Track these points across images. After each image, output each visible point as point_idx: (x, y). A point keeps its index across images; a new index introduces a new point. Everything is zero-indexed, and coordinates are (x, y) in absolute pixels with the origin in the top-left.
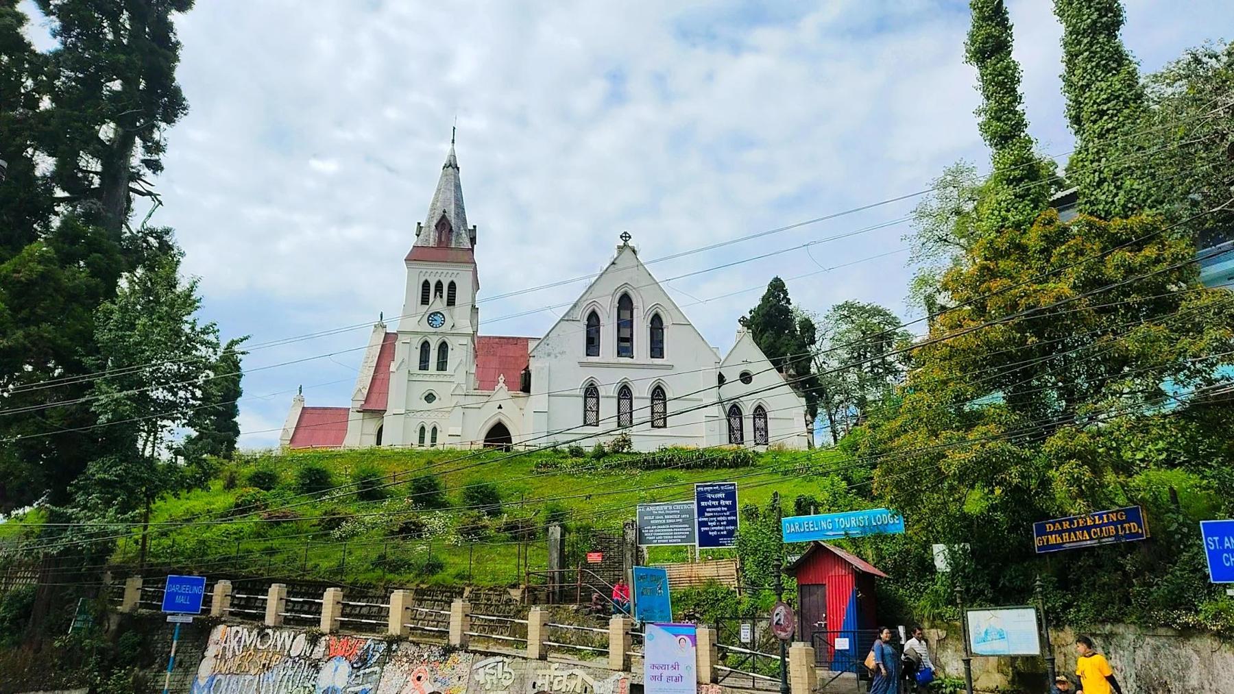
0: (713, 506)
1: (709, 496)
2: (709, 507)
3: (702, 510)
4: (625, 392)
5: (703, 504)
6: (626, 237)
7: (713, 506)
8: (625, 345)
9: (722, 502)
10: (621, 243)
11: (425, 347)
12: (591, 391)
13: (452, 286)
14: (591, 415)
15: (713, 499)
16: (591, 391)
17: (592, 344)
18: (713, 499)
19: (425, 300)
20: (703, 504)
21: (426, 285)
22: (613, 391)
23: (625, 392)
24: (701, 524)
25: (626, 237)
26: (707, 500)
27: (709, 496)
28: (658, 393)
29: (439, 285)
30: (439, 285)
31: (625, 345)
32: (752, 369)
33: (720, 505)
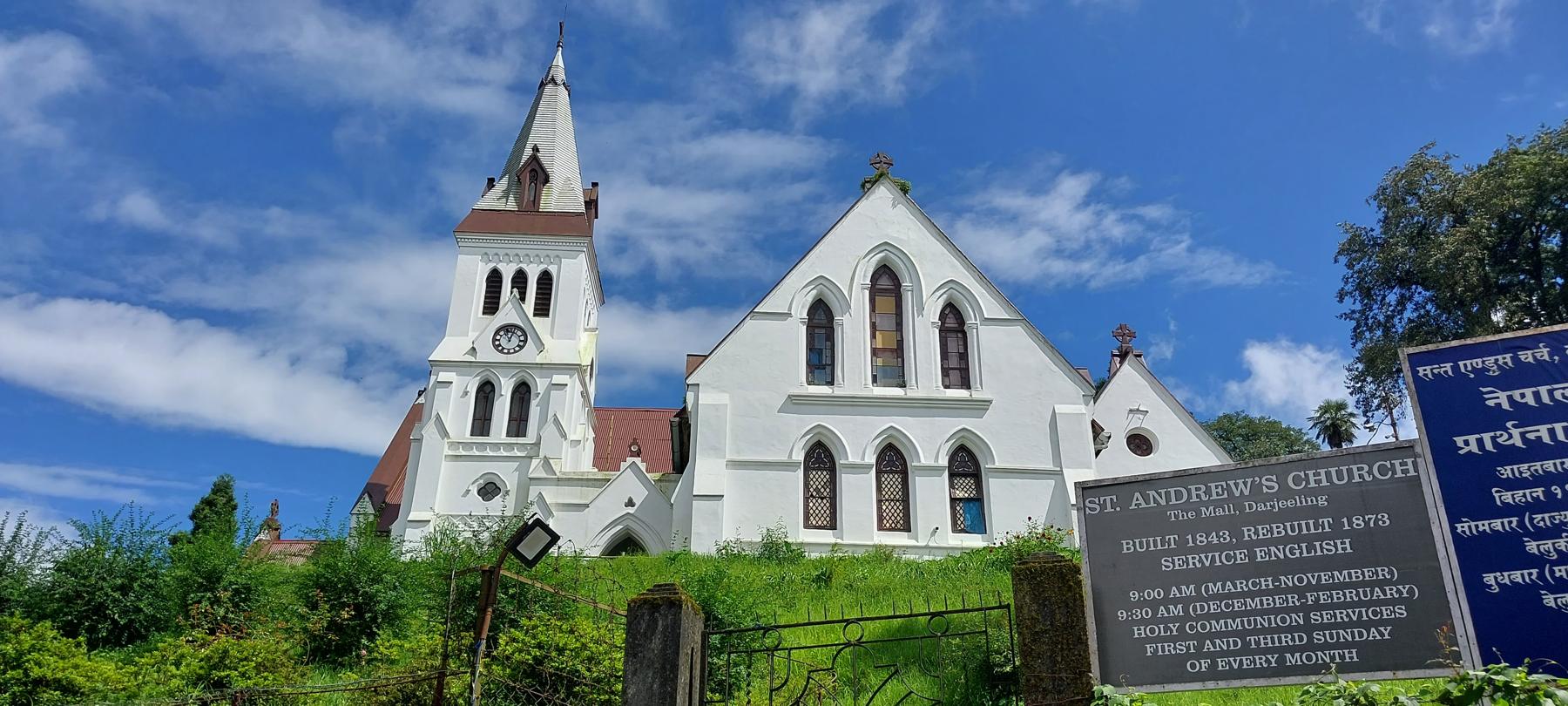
0: (1535, 450)
2: (1509, 455)
3: (1468, 487)
4: (893, 460)
5: (1468, 444)
8: (891, 361)
11: (486, 392)
12: (821, 458)
13: (546, 280)
14: (823, 503)
16: (821, 458)
17: (821, 362)
19: (491, 306)
20: (1468, 444)
21: (494, 279)
23: (893, 460)
28: (965, 463)
29: (520, 280)
30: (520, 280)
31: (891, 361)
32: (1148, 425)
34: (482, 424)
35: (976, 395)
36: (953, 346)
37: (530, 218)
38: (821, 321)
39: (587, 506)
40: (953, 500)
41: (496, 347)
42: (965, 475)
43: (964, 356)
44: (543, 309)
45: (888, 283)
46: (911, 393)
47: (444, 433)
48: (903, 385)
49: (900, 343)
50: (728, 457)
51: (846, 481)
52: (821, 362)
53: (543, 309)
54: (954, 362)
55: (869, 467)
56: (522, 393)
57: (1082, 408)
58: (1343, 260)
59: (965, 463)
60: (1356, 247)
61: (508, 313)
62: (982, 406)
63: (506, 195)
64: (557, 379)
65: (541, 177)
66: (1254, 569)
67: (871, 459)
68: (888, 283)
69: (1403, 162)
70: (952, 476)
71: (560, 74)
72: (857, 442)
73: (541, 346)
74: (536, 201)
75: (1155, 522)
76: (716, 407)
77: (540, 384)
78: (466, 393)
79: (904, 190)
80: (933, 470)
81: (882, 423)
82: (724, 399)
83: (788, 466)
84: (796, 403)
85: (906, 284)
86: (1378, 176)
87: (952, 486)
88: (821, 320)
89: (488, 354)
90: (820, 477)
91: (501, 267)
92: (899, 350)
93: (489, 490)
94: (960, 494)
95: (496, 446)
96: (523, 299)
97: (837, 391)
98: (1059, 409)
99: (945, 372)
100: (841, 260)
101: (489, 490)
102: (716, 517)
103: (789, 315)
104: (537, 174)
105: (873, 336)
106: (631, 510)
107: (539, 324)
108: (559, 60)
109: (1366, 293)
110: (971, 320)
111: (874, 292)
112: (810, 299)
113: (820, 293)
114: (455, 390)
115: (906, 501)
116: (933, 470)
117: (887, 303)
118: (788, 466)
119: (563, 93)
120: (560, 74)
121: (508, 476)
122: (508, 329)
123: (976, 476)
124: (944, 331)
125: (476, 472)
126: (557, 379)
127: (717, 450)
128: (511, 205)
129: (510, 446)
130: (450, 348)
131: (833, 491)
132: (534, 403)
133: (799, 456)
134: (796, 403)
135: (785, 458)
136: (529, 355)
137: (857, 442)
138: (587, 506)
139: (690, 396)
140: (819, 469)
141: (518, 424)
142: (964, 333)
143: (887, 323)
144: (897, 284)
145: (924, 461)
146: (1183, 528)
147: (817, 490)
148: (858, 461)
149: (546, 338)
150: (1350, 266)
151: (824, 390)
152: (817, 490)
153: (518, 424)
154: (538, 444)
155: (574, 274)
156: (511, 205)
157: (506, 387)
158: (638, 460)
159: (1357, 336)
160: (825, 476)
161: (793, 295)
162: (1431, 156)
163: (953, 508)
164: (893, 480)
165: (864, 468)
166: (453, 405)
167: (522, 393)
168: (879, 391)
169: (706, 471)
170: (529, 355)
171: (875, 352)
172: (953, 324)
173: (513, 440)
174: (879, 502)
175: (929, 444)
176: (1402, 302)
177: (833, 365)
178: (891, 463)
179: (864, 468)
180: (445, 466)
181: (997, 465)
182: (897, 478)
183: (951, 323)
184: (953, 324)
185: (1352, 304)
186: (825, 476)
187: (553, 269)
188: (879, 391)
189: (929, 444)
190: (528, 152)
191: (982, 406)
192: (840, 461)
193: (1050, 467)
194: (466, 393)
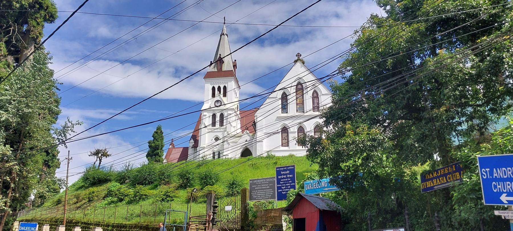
1: (282, 173)
2: (282, 178)
3: (279, 181)
5: (279, 177)
6: (299, 55)
7: (284, 178)
9: (288, 176)
10: (296, 58)
11: (214, 116)
13: (225, 88)
15: (284, 175)
17: (284, 108)
18: (284, 175)
19: (214, 95)
20: (279, 177)
21: (214, 88)
22: (295, 129)
24: (279, 188)
25: (299, 55)
26: (281, 175)
27: (282, 173)
29: (219, 88)
30: (219, 88)
33: (287, 178)
34: (214, 124)
36: (316, 101)
37: (220, 73)
38: (284, 97)
44: (225, 95)
52: (284, 108)
56: (222, 116)
61: (217, 98)
64: (230, 112)
66: (262, 189)
68: (300, 88)
74: (221, 68)
75: (255, 184)
77: (225, 114)
88: (284, 97)
90: (285, 135)
91: (215, 86)
96: (220, 93)
101: (217, 139)
102: (262, 146)
107: (225, 100)
122: (217, 101)
125: (213, 135)
128: (216, 70)
130: (205, 106)
134: (279, 119)
141: (222, 124)
146: (257, 185)
151: (285, 115)
153: (222, 124)
156: (216, 70)
166: (207, 121)
167: (222, 116)
168: (298, 114)
183: (315, 95)
188: (298, 114)
190: (218, 56)
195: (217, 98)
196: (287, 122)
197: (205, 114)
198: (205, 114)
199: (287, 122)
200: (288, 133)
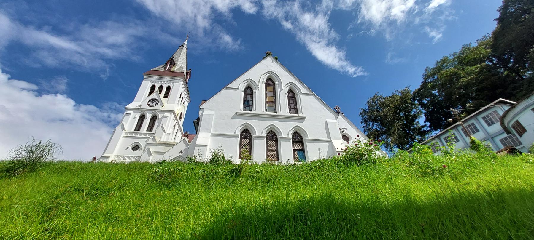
4: (272, 136)
8: (272, 103)
11: (142, 118)
12: (246, 135)
13: (169, 89)
16: (246, 135)
17: (248, 103)
21: (153, 87)
23: (272, 136)
28: (298, 138)
29: (161, 88)
30: (161, 88)
31: (272, 103)
34: (139, 127)
35: (300, 115)
36: (292, 102)
38: (249, 92)
39: (165, 153)
40: (294, 150)
41: (148, 105)
42: (298, 142)
43: (296, 105)
44: (166, 96)
45: (271, 83)
46: (278, 114)
47: (123, 129)
48: (276, 112)
49: (275, 100)
50: (212, 132)
51: (255, 142)
52: (248, 103)
53: (166, 96)
54: (292, 106)
55: (264, 137)
57: (335, 121)
58: (361, 116)
59: (298, 138)
60: (363, 113)
61: (154, 96)
62: (303, 119)
63: (162, 68)
64: (166, 114)
65: (173, 63)
67: (265, 135)
68: (271, 83)
69: (372, 96)
70: (293, 142)
71: (185, 45)
72: (260, 129)
73: (162, 105)
76: (209, 115)
77: (160, 116)
78: (135, 117)
79: (276, 59)
80: (287, 139)
81: (269, 123)
82: (213, 113)
83: (234, 136)
84: (238, 115)
85: (277, 82)
86: (367, 100)
87: (293, 146)
88: (249, 92)
89: (145, 106)
90: (245, 141)
91: (156, 84)
92: (274, 102)
93: (136, 148)
94: (296, 148)
95: (141, 134)
96: (160, 93)
97: (253, 112)
98: (328, 121)
99: (290, 109)
100: (258, 73)
101: (136, 148)
103: (238, 89)
104: (173, 64)
105: (266, 98)
106: (181, 154)
107: (164, 100)
108: (186, 42)
109: (366, 122)
110: (297, 93)
111: (267, 85)
112: (246, 85)
113: (249, 84)
114: (131, 117)
115: (277, 150)
116: (287, 139)
117: (270, 88)
118: (234, 136)
119: (185, 50)
120: (185, 45)
121: (142, 143)
122: (153, 100)
123: (302, 142)
124: (289, 98)
126: (166, 114)
127: (207, 130)
128: (163, 69)
129: (146, 134)
131: (251, 146)
132: (157, 121)
133: (239, 133)
134: (238, 115)
135: (233, 133)
136: (158, 107)
137: (260, 129)
138: (165, 153)
139: (200, 112)
140: (246, 138)
141: (151, 128)
142: (295, 98)
143: (271, 94)
144: (274, 83)
145: (283, 136)
147: (245, 146)
148: (260, 135)
149: (165, 104)
150: (362, 117)
152: (245, 146)
153: (151, 128)
154: (155, 134)
155: (179, 88)
156: (163, 69)
157: (149, 117)
158: (186, 138)
159: (365, 131)
160: (248, 141)
161: (240, 83)
162: (378, 95)
163: (294, 153)
164: (272, 143)
165: (262, 138)
168: (267, 113)
169: (203, 137)
170: (158, 107)
171: (266, 102)
172: (292, 96)
173: (148, 132)
174: (267, 150)
175: (285, 130)
176: (373, 125)
177: (252, 105)
178: (272, 137)
179: (262, 138)
180: (121, 140)
181: (309, 138)
182: (274, 142)
183: (291, 95)
184: (292, 96)
185: (363, 125)
186: (248, 141)
187: (171, 86)
188: (267, 113)
189: (285, 130)
191: (303, 119)
192: (253, 135)
193: (327, 139)
194: (135, 117)
195: (154, 96)
196: (250, 122)
197: (128, 112)
198: (128, 112)
199: (250, 122)
200: (251, 139)
